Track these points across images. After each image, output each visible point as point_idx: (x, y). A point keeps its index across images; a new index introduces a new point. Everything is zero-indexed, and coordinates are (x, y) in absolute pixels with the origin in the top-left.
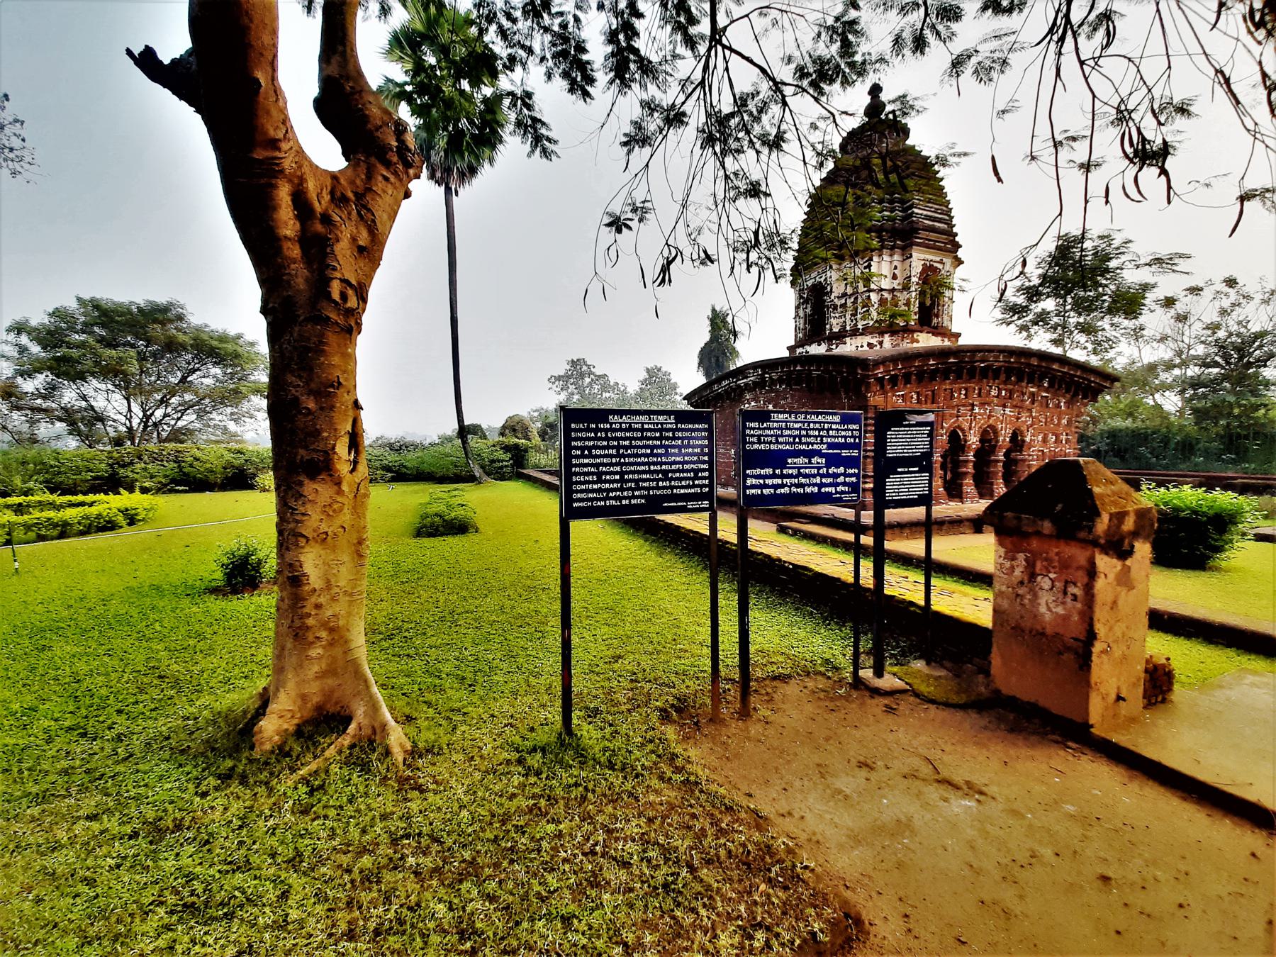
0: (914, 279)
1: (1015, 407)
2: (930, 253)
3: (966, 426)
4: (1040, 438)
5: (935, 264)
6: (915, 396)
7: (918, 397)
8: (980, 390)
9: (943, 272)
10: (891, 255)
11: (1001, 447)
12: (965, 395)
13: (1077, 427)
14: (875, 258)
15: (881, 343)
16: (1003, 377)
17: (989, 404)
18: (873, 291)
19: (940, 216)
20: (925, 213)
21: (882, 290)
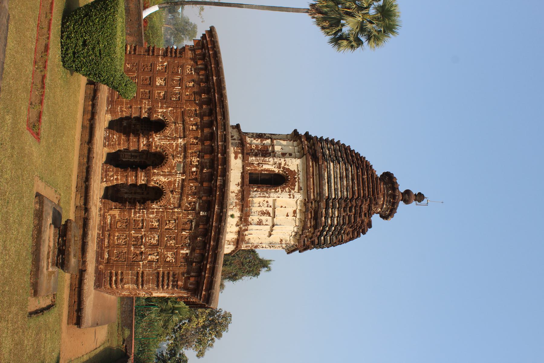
0: (282, 160)
1: (183, 186)
2: (303, 176)
3: (168, 132)
4: (156, 224)
5: (297, 183)
6: (191, 84)
7: (190, 87)
8: (197, 143)
9: (293, 191)
10: (298, 152)
11: (148, 176)
12: (192, 130)
13: (163, 273)
14: (295, 143)
15: (234, 139)
16: (207, 157)
17: (185, 157)
18: (272, 141)
19: (333, 188)
20: (332, 172)
21: (273, 146)
